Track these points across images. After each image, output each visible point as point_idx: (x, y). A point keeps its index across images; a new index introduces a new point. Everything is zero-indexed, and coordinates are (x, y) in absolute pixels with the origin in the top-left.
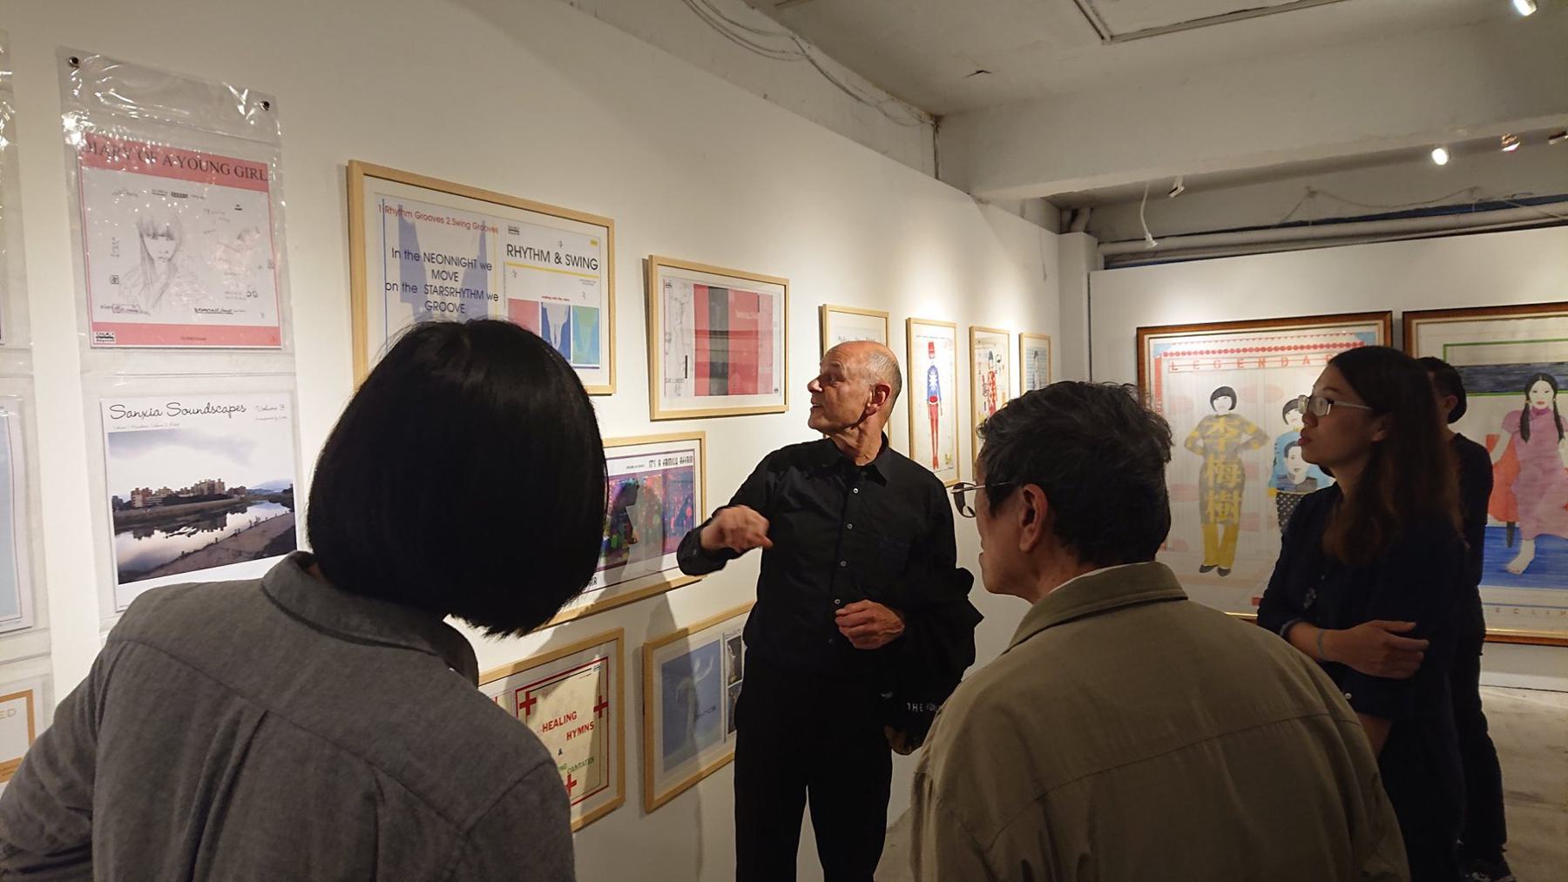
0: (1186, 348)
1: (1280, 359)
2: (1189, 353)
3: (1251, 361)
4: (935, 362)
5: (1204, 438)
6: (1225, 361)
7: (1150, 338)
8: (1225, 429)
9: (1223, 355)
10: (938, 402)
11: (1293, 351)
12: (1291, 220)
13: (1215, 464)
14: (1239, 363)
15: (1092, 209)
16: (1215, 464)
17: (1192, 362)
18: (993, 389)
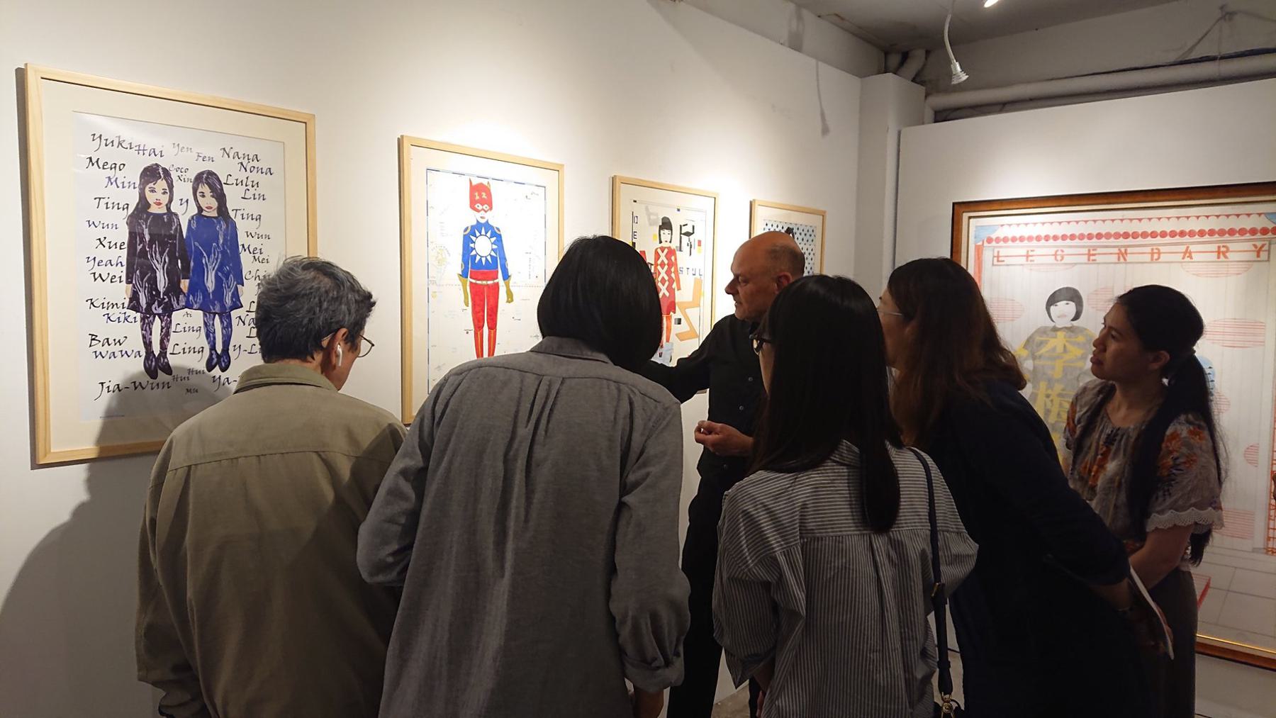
0: (1017, 232)
1: (1148, 250)
2: (1022, 239)
3: (1107, 256)
4: (494, 218)
5: (1034, 358)
6: (1067, 251)
7: (970, 218)
8: (1065, 346)
9: (1068, 242)
10: (500, 280)
11: (1168, 239)
12: (1193, 56)
13: (1048, 396)
14: (1089, 255)
15: (928, 52)
16: (1048, 396)
17: (1024, 252)
18: (668, 273)
